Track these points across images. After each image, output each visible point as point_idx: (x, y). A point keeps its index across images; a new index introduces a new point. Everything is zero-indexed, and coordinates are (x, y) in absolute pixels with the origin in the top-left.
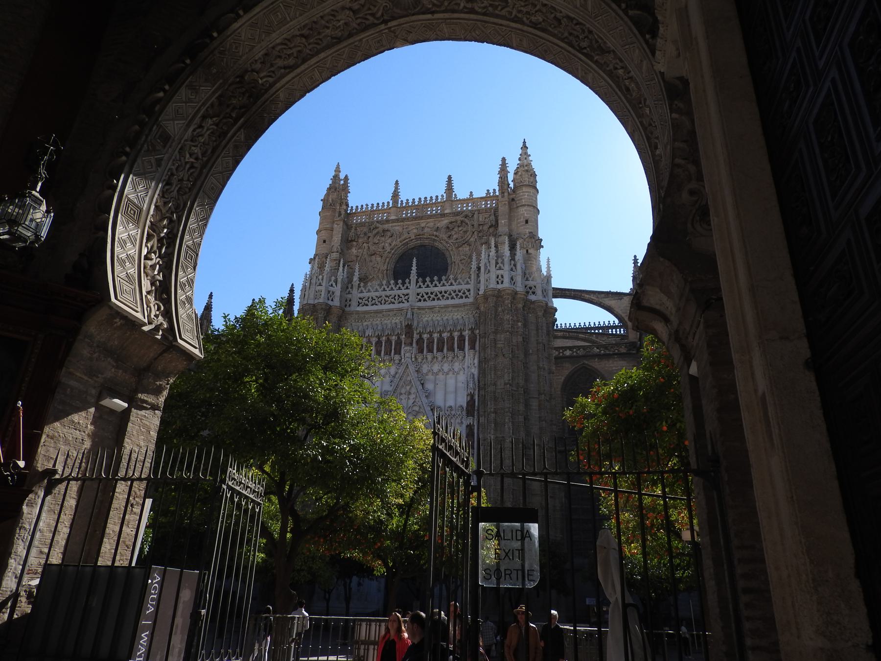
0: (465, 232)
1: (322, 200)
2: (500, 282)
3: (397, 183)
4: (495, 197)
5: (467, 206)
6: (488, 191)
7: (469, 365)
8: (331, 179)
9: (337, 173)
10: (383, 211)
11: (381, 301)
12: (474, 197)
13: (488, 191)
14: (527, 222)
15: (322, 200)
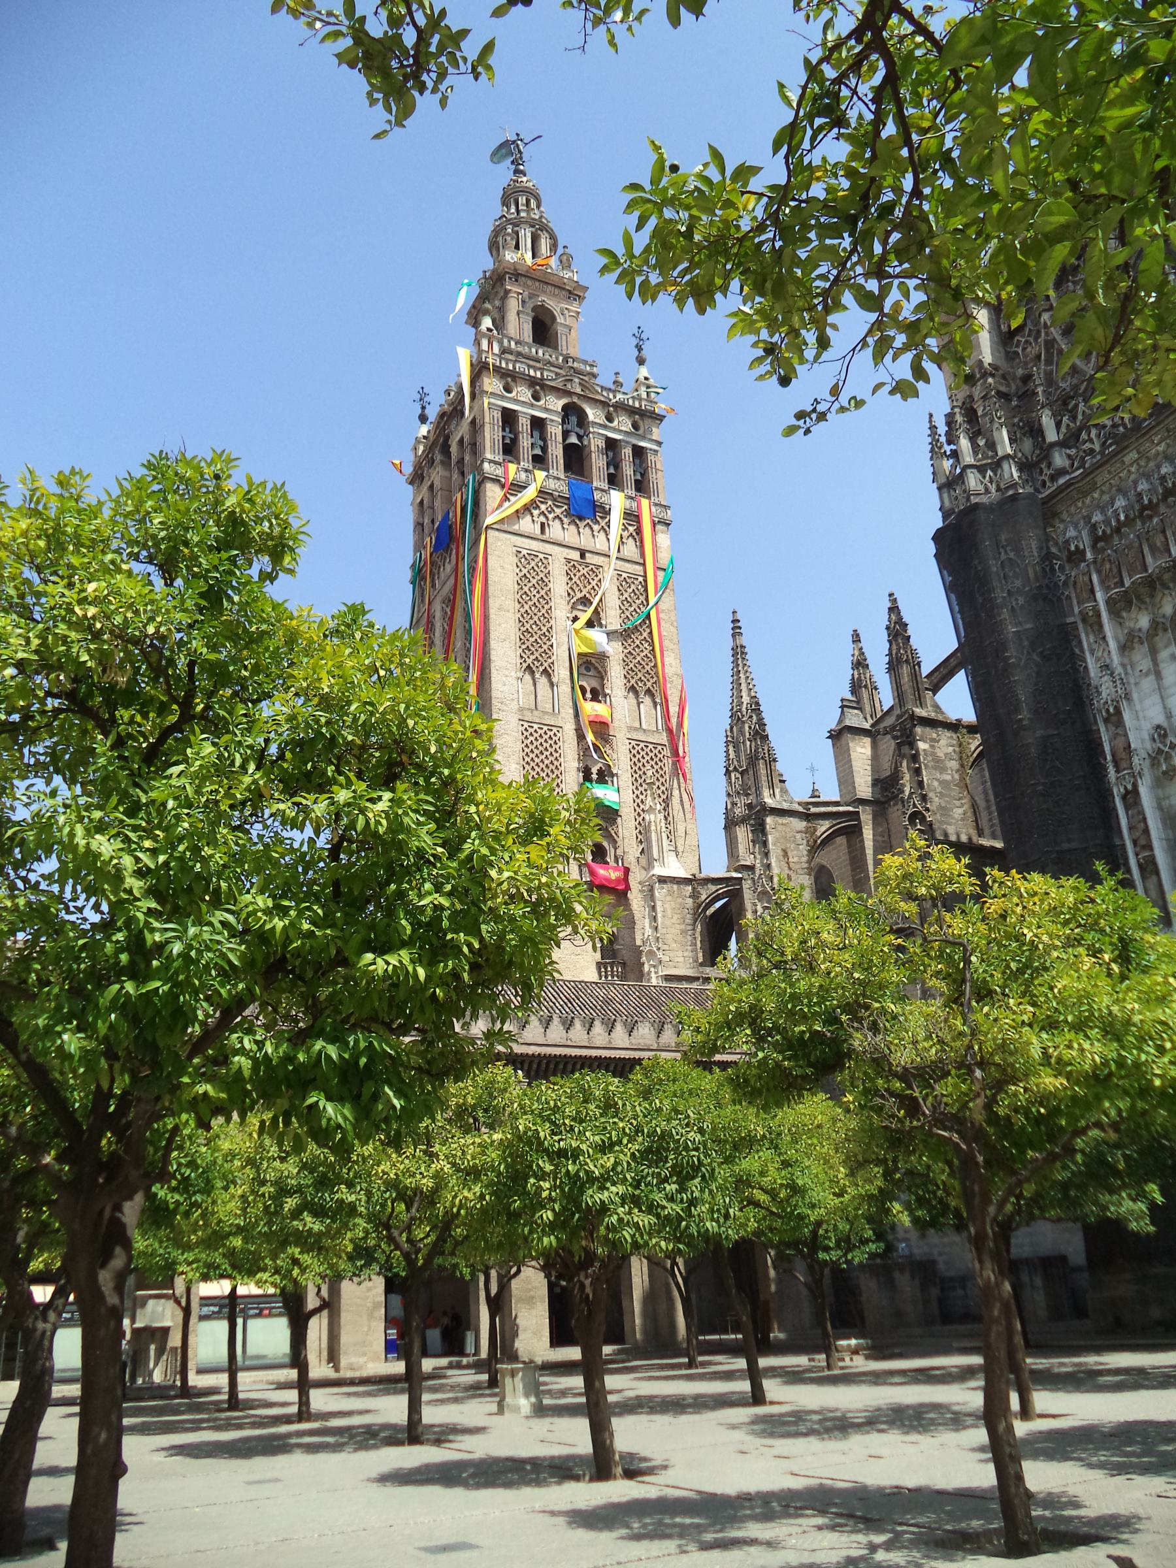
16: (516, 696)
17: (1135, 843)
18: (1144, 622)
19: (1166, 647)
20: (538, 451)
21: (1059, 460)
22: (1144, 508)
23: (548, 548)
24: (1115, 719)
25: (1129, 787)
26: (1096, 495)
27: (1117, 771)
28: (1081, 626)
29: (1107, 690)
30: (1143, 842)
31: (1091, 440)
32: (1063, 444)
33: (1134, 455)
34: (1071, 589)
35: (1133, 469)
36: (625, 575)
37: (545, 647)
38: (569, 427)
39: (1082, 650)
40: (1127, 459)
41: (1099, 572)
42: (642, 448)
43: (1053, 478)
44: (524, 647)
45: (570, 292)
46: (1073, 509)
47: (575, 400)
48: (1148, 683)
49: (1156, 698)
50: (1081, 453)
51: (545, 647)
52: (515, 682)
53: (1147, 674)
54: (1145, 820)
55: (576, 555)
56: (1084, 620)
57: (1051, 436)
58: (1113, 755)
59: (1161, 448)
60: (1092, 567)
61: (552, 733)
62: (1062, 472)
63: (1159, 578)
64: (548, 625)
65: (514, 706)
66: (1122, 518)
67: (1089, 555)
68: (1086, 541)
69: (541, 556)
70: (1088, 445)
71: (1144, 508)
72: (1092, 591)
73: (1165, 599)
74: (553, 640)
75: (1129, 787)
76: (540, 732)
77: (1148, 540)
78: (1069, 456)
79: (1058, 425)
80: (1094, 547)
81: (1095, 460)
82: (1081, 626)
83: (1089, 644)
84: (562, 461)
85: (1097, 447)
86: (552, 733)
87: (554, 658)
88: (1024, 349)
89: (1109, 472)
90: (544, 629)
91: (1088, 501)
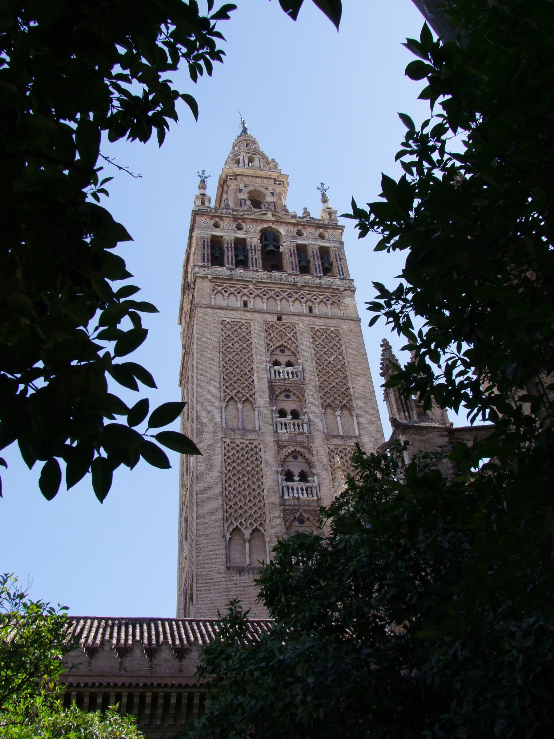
16: (219, 420)
20: (241, 258)
23: (250, 316)
36: (317, 327)
37: (247, 383)
38: (267, 243)
42: (328, 248)
44: (227, 384)
45: (275, 180)
47: (270, 224)
51: (247, 383)
52: (219, 410)
55: (274, 318)
61: (253, 446)
64: (250, 368)
65: (218, 428)
69: (243, 321)
74: (255, 378)
76: (241, 446)
84: (260, 262)
86: (253, 446)
87: (254, 390)
90: (246, 371)
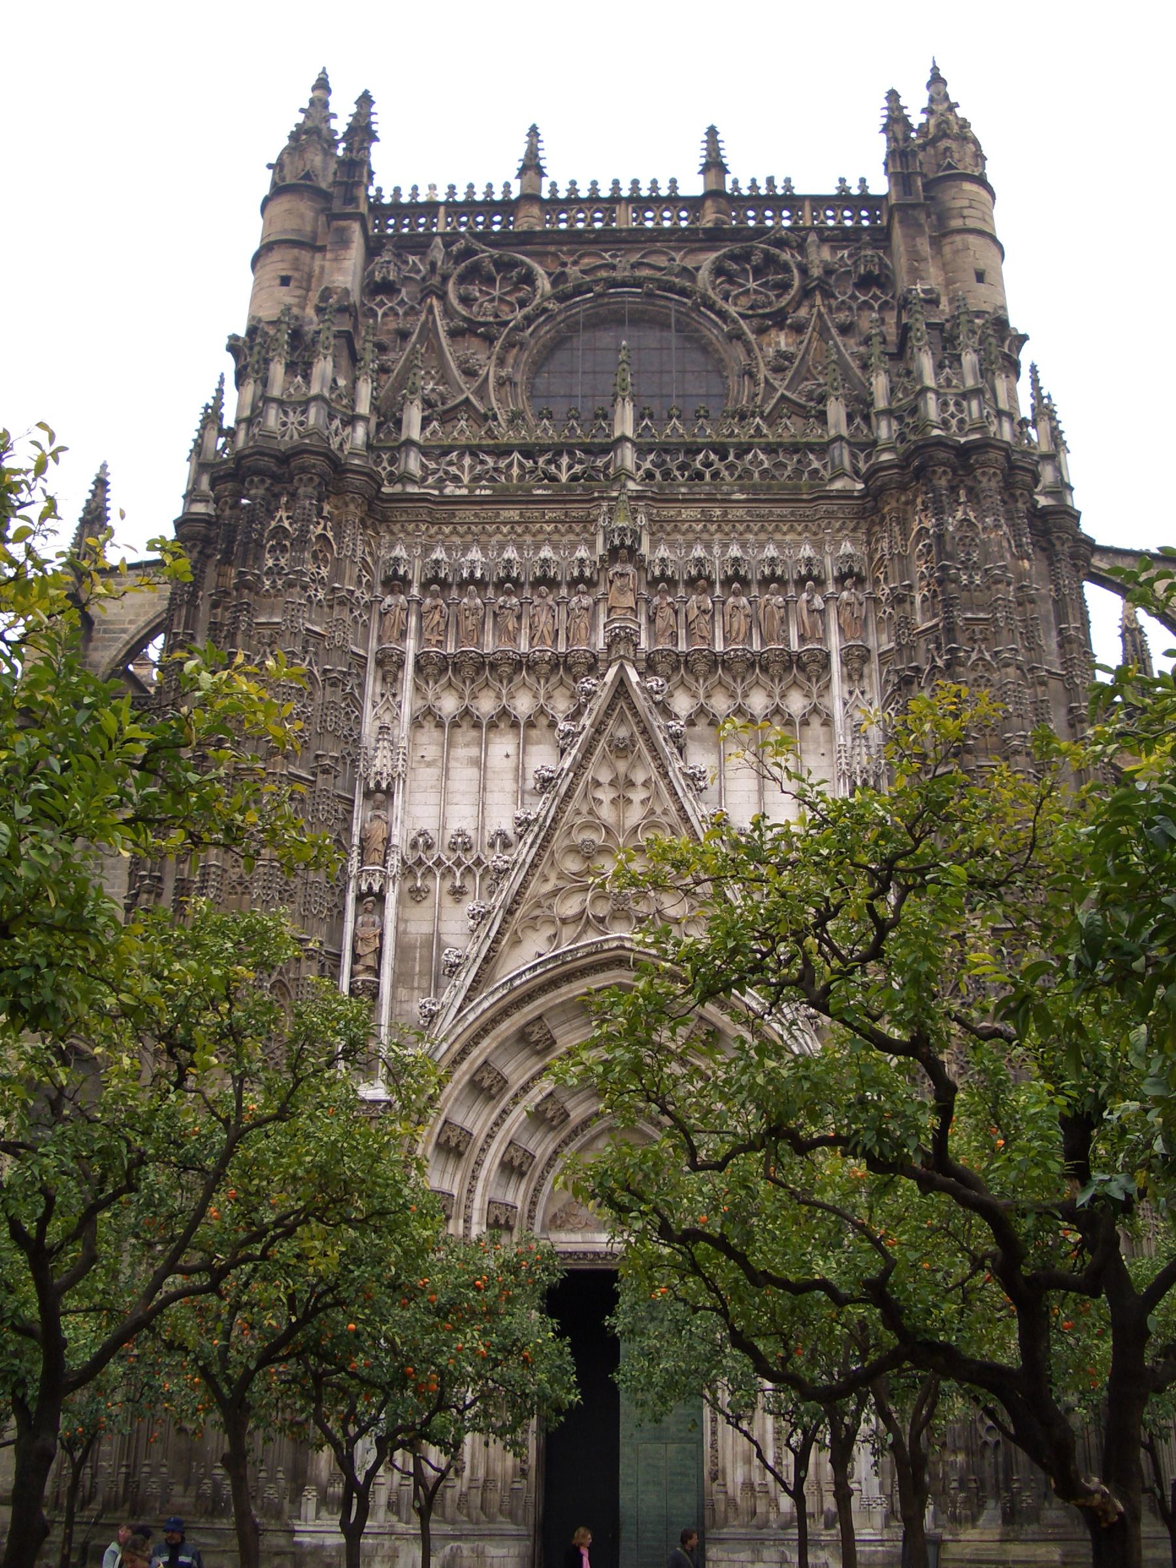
0: (784, 287)
1: (270, 166)
2: (954, 422)
3: (534, 132)
4: (866, 200)
5: (778, 216)
6: (842, 180)
7: (847, 696)
8: (302, 110)
9: (318, 93)
10: (489, 207)
11: (510, 465)
12: (797, 192)
13: (842, 180)
14: (980, 277)
15: (270, 166)
17: (356, 958)
18: (449, 705)
19: (467, 745)
21: (413, 463)
22: (508, 578)
24: (380, 795)
25: (376, 888)
26: (447, 530)
27: (362, 862)
28: (371, 665)
29: (382, 761)
30: (370, 961)
31: (461, 468)
32: (425, 451)
33: (514, 515)
34: (376, 618)
35: (505, 530)
39: (362, 694)
40: (505, 514)
41: (420, 617)
43: (393, 479)
46: (411, 527)
48: (427, 776)
49: (433, 798)
50: (441, 473)
53: (429, 765)
54: (381, 936)
56: (379, 663)
57: (413, 428)
58: (361, 840)
59: (549, 528)
60: (414, 606)
62: (407, 478)
63: (493, 666)
66: (478, 574)
67: (415, 591)
68: (416, 576)
70: (453, 470)
71: (508, 578)
72: (403, 635)
73: (485, 692)
75: (376, 888)
77: (495, 615)
78: (424, 467)
79: (425, 422)
80: (425, 586)
81: (458, 492)
82: (371, 665)
83: (374, 694)
85: (466, 479)
88: (385, 315)
89: (476, 515)
91: (433, 530)
